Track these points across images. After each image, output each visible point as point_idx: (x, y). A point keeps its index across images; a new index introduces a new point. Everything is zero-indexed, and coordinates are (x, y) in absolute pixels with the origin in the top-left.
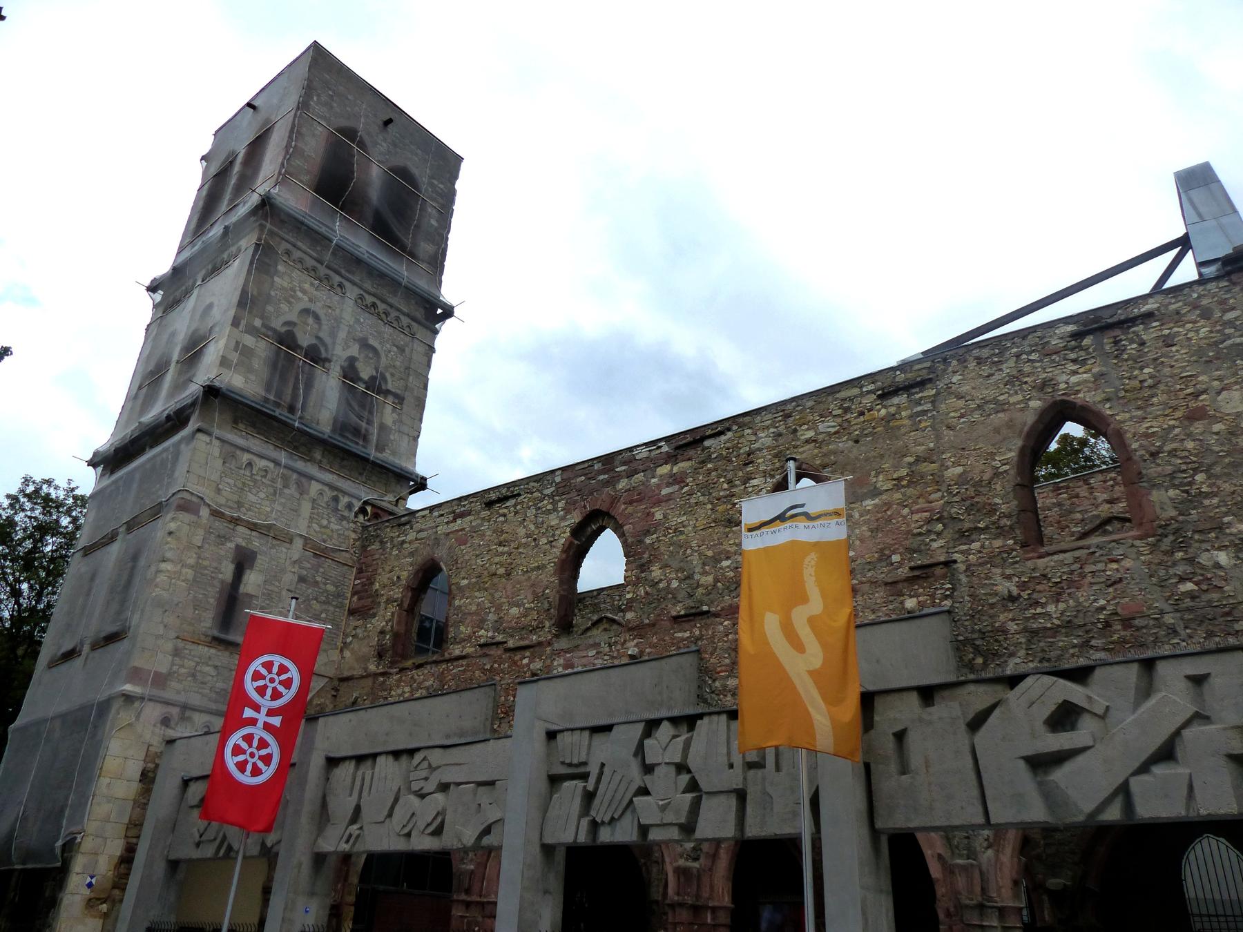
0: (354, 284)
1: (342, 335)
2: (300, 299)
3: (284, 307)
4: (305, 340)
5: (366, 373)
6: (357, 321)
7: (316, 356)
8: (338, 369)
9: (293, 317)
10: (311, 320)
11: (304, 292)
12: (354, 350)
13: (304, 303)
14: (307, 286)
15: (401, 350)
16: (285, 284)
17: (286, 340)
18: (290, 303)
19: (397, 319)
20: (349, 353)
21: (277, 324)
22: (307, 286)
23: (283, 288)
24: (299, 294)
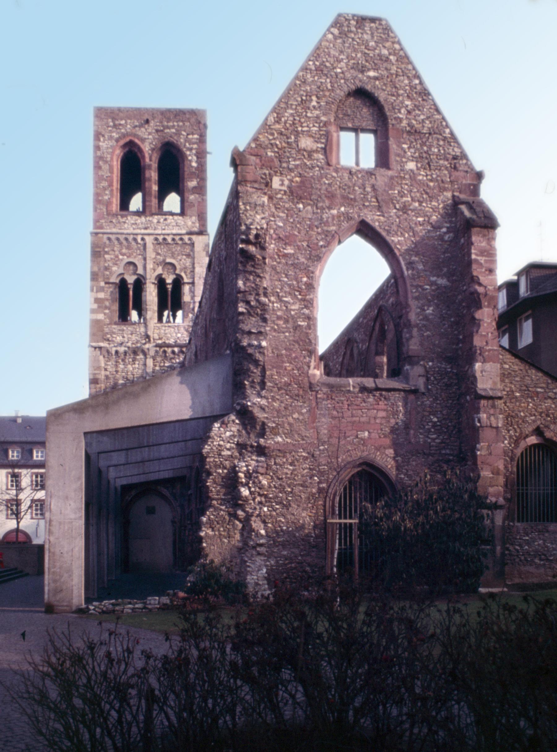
0: (149, 234)
1: (150, 266)
2: (122, 260)
3: (115, 268)
4: (131, 279)
5: (169, 280)
6: (158, 254)
7: (139, 284)
8: (152, 286)
9: (121, 271)
10: (131, 267)
11: (123, 255)
12: (159, 270)
13: (126, 260)
14: (124, 251)
15: (188, 256)
16: (112, 257)
17: (123, 285)
18: (116, 264)
19: (181, 239)
20: (157, 273)
21: (115, 279)
22: (124, 251)
23: (112, 259)
24: (121, 257)
